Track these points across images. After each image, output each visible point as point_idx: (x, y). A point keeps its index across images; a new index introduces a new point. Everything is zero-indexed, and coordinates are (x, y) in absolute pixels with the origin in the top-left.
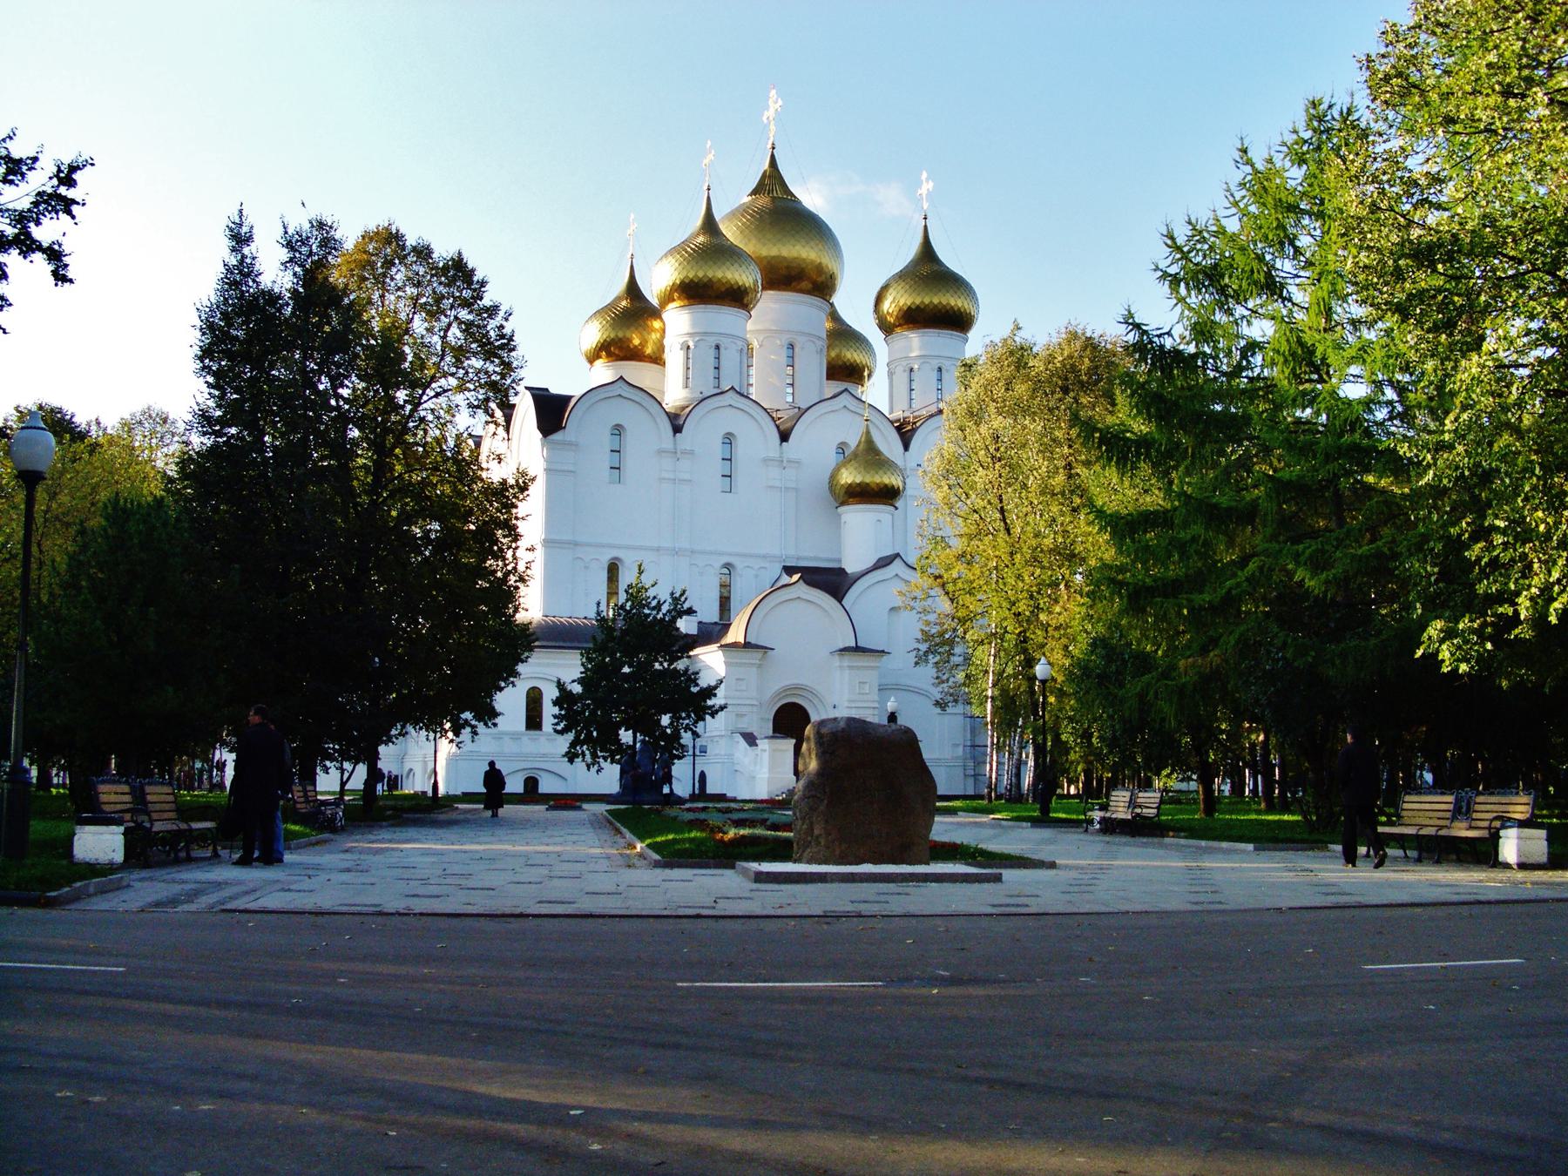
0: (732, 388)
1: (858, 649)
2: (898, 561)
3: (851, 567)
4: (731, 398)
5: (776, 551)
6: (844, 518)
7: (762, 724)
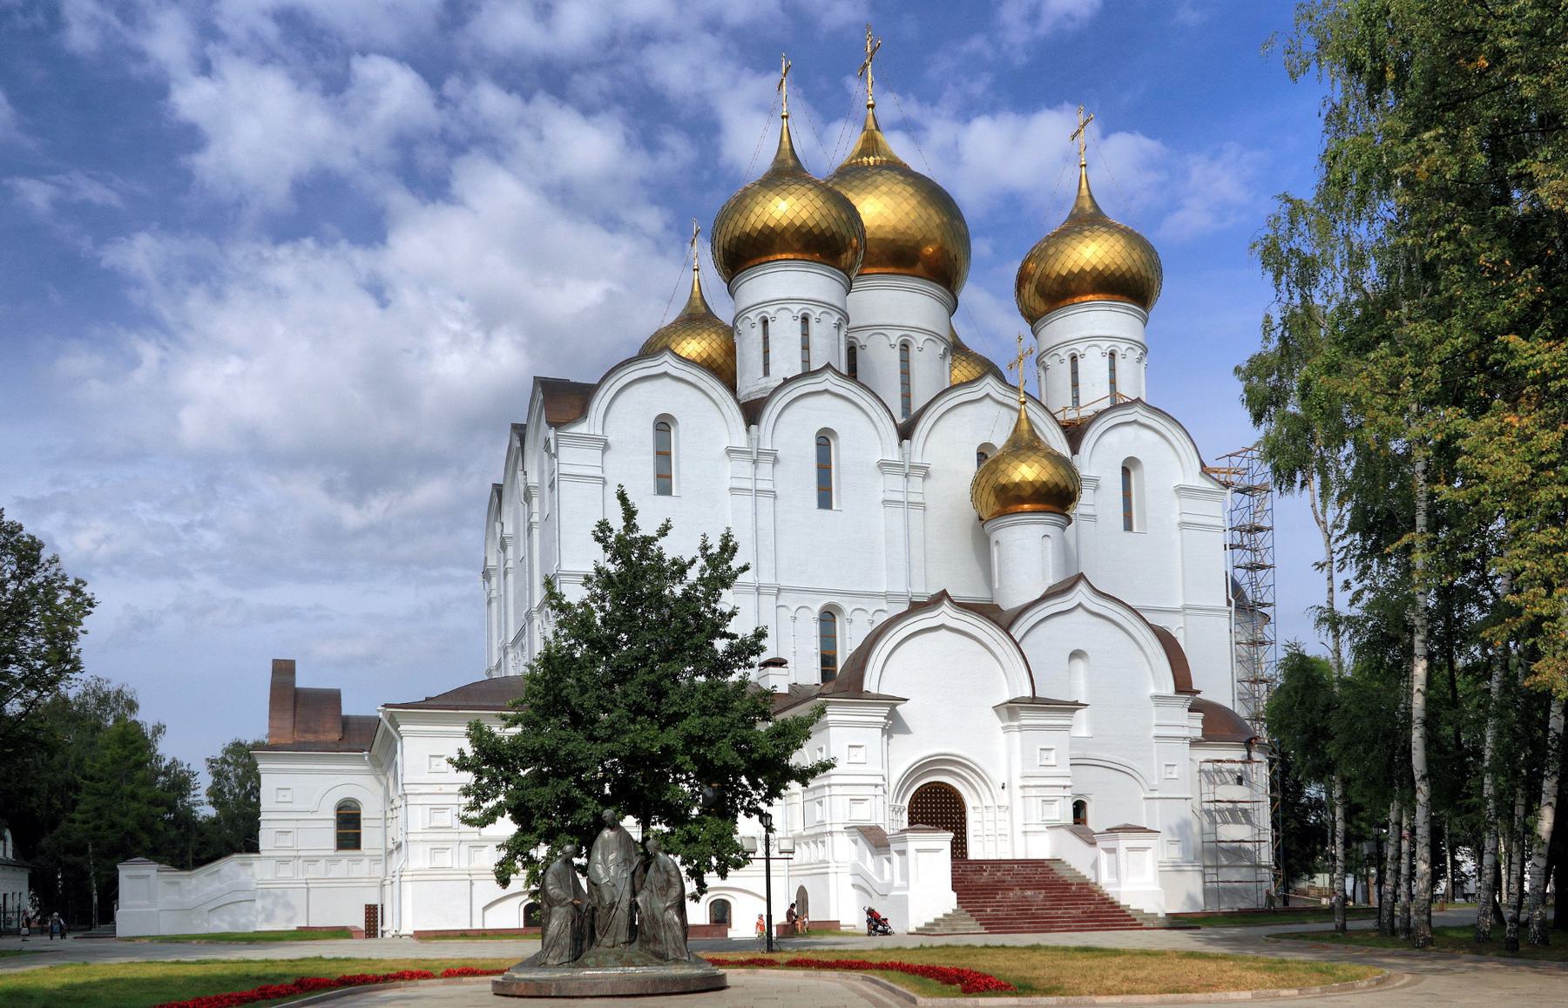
0: (828, 366)
1: (1036, 703)
2: (1082, 586)
3: (1011, 600)
4: (829, 381)
5: (901, 588)
6: (994, 538)
7: (889, 814)
